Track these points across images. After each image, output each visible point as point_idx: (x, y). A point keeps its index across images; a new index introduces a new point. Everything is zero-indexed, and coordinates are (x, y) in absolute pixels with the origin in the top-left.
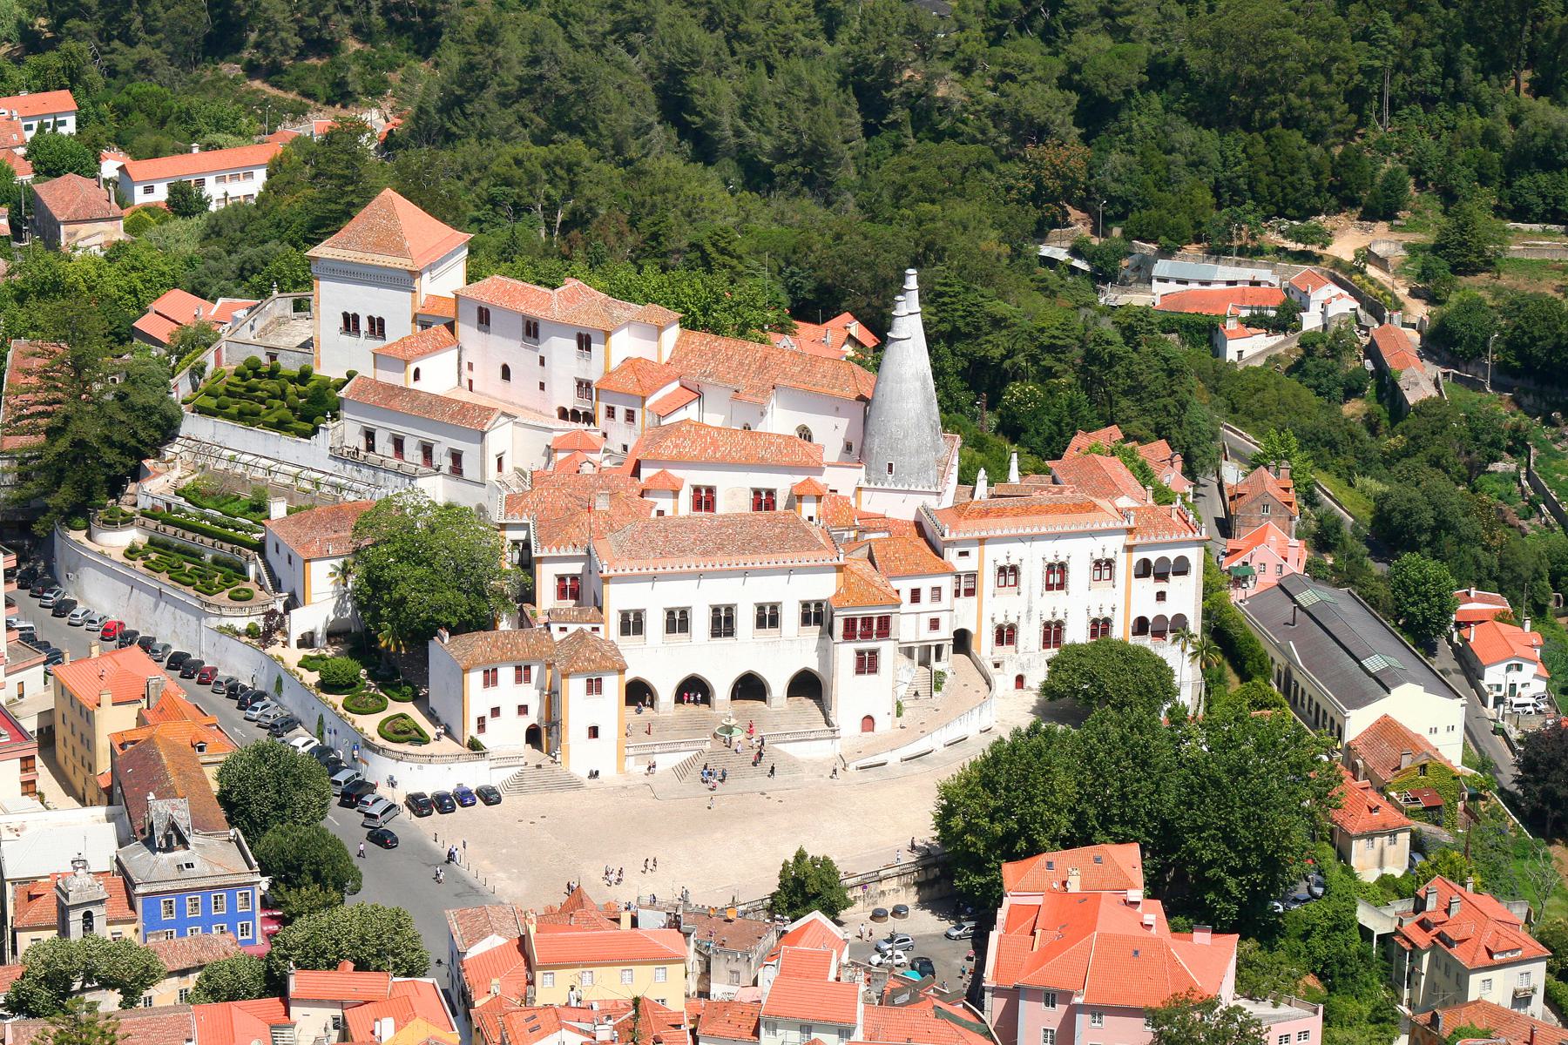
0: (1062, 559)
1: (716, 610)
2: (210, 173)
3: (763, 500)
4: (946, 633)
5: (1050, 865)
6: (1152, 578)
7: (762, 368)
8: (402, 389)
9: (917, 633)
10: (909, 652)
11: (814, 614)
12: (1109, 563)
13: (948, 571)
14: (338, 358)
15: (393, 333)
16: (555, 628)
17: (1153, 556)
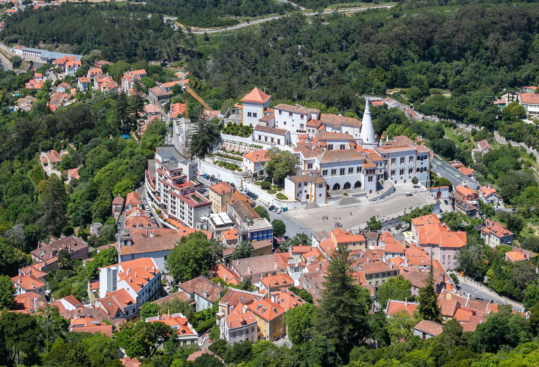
3: (343, 147)
4: (383, 173)
14: (247, 122)
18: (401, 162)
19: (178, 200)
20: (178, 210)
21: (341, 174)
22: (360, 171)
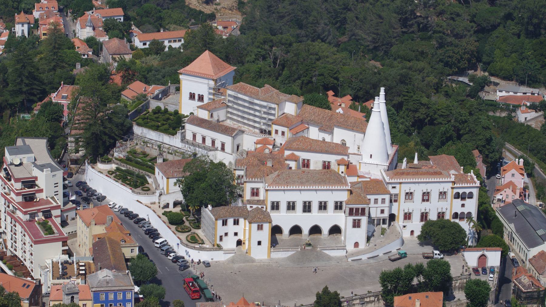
0: (428, 191)
1: (305, 203)
2: (166, 39)
3: (326, 166)
4: (386, 215)
5: (410, 298)
6: (460, 199)
7: (330, 119)
8: (206, 120)
9: (376, 214)
11: (338, 206)
13: (387, 193)
14: (187, 107)
15: (206, 100)
16: (248, 206)
17: (461, 191)
18: (423, 200)
19: (19, 228)
20: (19, 245)
21: (304, 211)
22: (341, 208)
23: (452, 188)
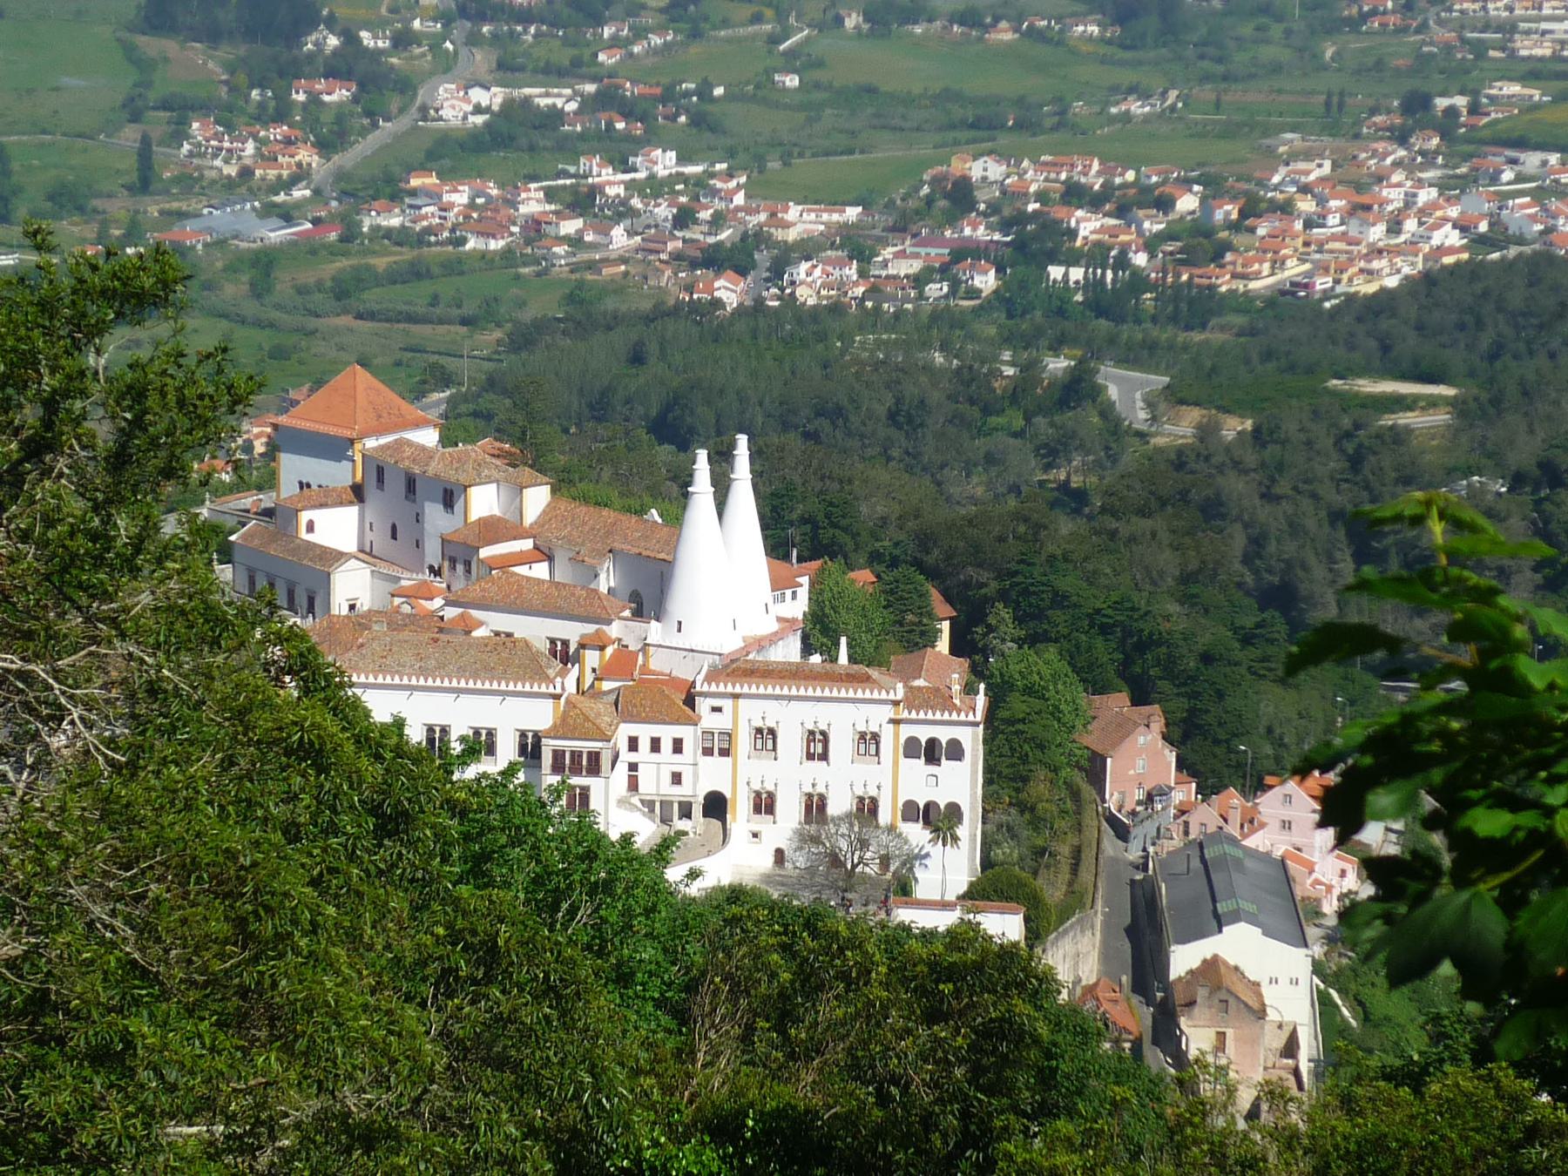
10: (650, 805)
12: (876, 737)
17: (923, 734)
23: (896, 722)
